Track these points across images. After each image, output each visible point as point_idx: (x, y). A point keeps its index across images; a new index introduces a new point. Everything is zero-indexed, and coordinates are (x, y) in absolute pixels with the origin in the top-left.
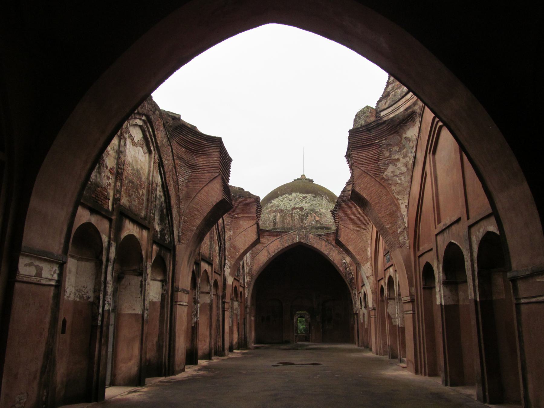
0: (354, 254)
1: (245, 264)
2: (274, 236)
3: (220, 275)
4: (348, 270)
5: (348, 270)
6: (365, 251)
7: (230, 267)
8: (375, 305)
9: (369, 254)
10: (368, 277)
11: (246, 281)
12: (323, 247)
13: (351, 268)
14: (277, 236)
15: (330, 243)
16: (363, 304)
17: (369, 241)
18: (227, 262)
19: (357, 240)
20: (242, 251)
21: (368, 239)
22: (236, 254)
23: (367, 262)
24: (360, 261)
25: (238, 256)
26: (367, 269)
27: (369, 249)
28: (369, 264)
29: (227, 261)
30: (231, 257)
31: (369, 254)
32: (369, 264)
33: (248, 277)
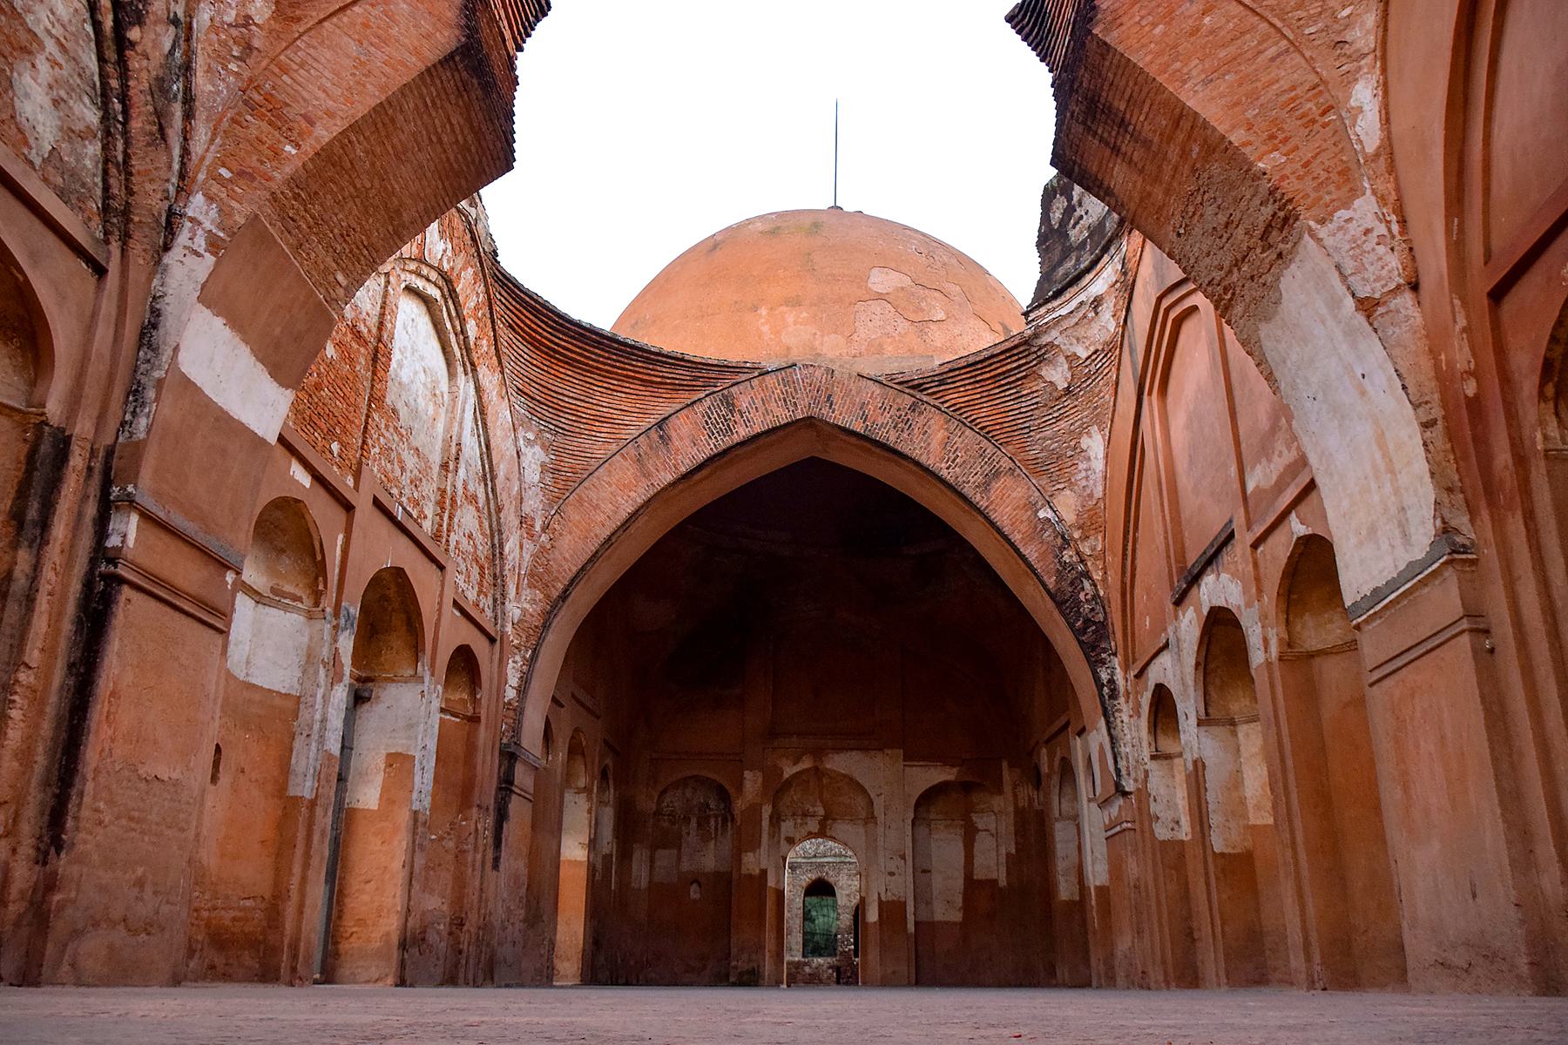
0: (1236, 137)
1: (510, 518)
2: (677, 387)
3: (100, 271)
4: (1068, 556)
5: (1068, 556)
6: (1328, 110)
7: (214, 244)
8: (1461, 521)
9: (1368, 130)
10: (1367, 307)
11: (514, 610)
12: (934, 442)
13: (1085, 549)
14: (692, 388)
15: (971, 424)
16: (1188, 706)
17: (1363, 35)
18: (197, 205)
19: (1251, 41)
20: (324, 133)
21: (1349, 23)
22: (277, 153)
23: (1355, 192)
24: (1290, 187)
25: (288, 170)
26: (1356, 244)
27: (1364, 95)
28: (1365, 209)
29: (198, 199)
30: (240, 174)
31: (1368, 130)
32: (1365, 209)
33: (527, 593)
